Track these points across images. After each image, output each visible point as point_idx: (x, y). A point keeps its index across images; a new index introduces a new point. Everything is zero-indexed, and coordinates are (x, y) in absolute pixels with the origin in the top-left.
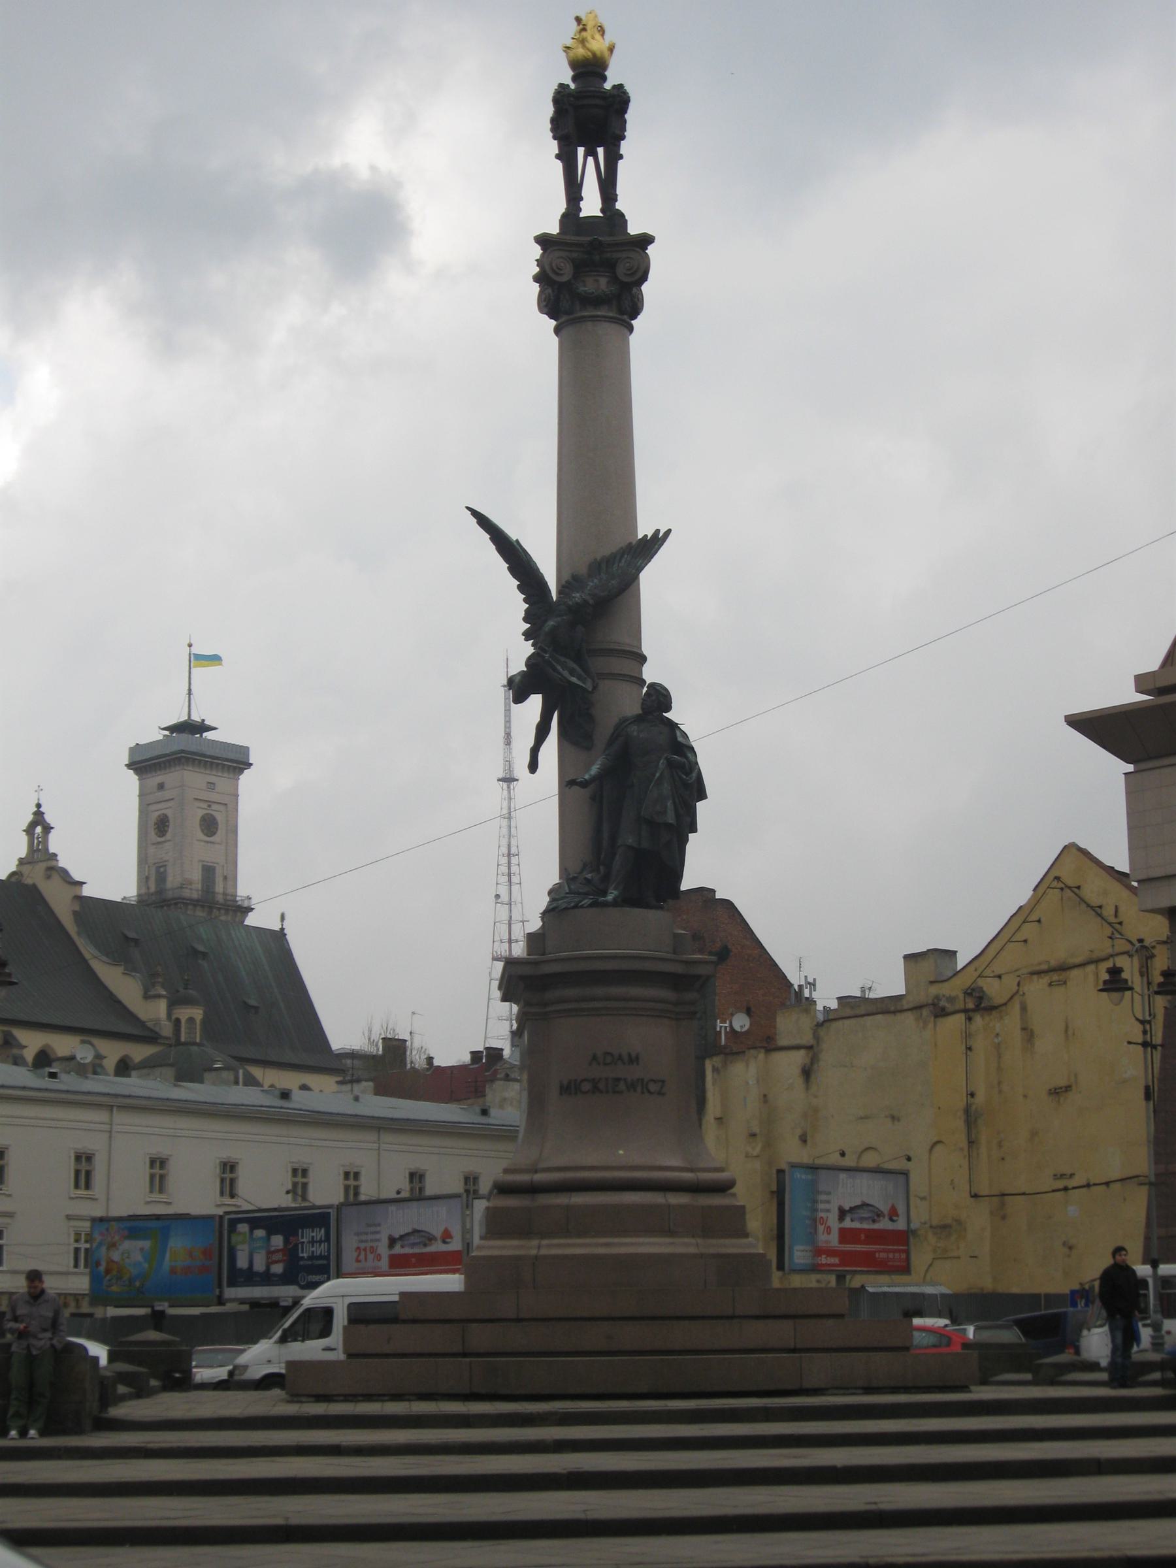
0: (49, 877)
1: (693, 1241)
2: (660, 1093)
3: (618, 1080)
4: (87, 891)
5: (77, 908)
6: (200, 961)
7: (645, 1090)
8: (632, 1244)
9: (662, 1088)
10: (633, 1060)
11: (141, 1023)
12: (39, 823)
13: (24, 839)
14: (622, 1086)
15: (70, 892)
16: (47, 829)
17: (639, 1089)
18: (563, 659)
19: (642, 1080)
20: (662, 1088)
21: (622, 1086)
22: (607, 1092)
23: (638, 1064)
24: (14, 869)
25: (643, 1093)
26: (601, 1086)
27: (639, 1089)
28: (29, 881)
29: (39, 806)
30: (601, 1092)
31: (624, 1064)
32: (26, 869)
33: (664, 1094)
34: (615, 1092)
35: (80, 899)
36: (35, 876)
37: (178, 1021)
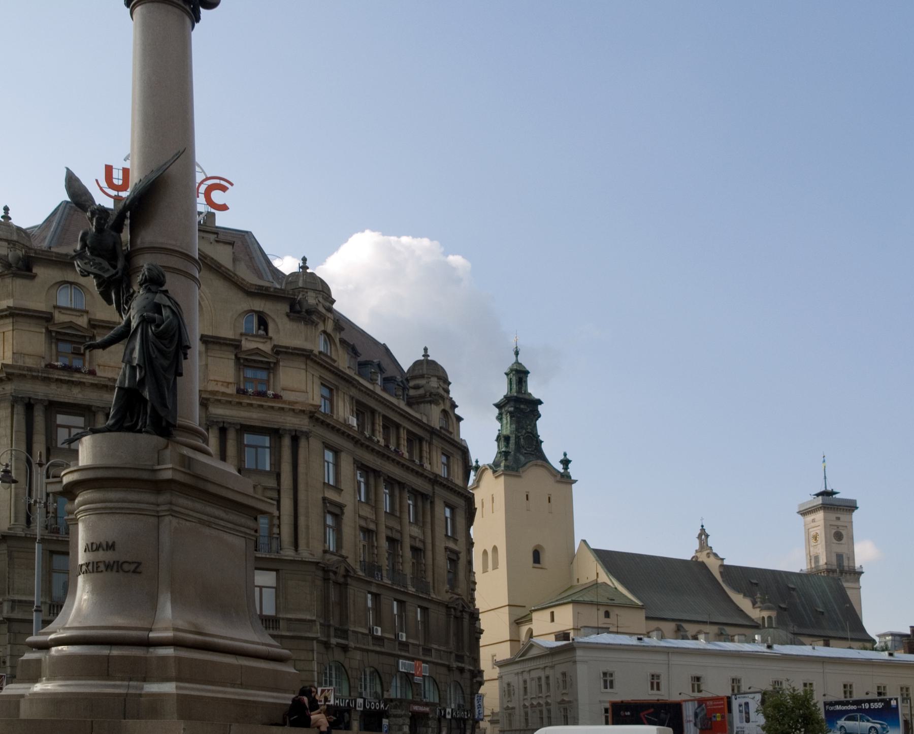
0: (709, 557)
3: (97, 563)
4: (726, 563)
5: (722, 570)
6: (792, 592)
7: (120, 569)
10: (111, 547)
11: (753, 620)
12: (703, 535)
13: (697, 541)
14: (102, 567)
15: (719, 562)
16: (707, 536)
17: (115, 567)
20: (137, 568)
22: (93, 572)
23: (114, 550)
24: (694, 555)
27: (115, 567)
28: (700, 560)
29: (702, 526)
31: (103, 550)
32: (698, 555)
34: (97, 572)
35: (722, 566)
36: (702, 557)
37: (763, 618)
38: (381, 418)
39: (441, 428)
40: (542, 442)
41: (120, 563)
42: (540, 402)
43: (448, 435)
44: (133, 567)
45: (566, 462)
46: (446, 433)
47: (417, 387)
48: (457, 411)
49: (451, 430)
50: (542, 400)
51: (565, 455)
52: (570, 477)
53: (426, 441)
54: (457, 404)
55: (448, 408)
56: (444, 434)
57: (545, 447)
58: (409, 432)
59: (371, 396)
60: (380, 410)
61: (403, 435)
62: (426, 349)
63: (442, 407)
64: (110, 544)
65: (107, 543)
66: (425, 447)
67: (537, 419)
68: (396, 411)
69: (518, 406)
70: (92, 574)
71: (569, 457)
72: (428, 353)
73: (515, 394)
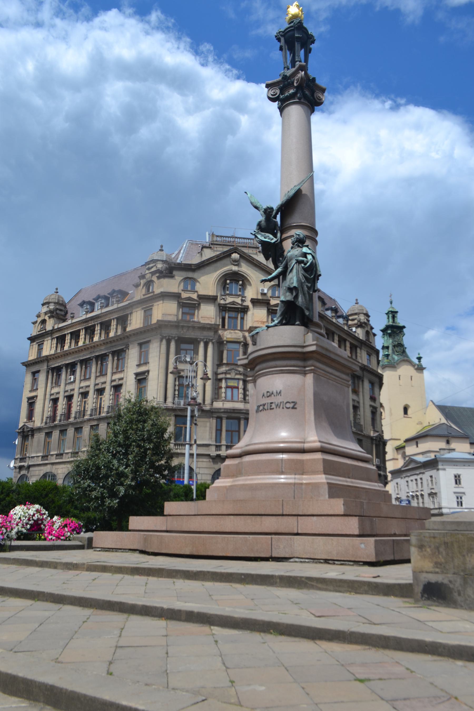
1: (293, 476)
2: (293, 408)
8: (261, 479)
9: (294, 405)
10: (279, 393)
18: (263, 233)
19: (283, 402)
20: (294, 405)
21: (273, 406)
23: (281, 395)
25: (283, 408)
26: (266, 407)
30: (266, 410)
31: (274, 396)
33: (296, 408)
34: (271, 409)
38: (337, 336)
39: (366, 340)
40: (406, 348)
41: (285, 402)
42: (404, 327)
43: (370, 343)
44: (291, 405)
45: (419, 359)
46: (369, 343)
47: (353, 320)
48: (374, 331)
49: (371, 341)
50: (406, 326)
51: (419, 354)
52: (421, 365)
53: (359, 348)
54: (373, 327)
55: (369, 330)
56: (368, 344)
57: (407, 351)
58: (351, 344)
59: (332, 325)
60: (336, 332)
61: (348, 345)
62: (357, 300)
63: (366, 329)
64: (278, 392)
65: (277, 393)
66: (358, 350)
67: (403, 336)
68: (345, 332)
69: (393, 330)
70: (267, 411)
71: (421, 355)
72: (358, 302)
73: (391, 324)
